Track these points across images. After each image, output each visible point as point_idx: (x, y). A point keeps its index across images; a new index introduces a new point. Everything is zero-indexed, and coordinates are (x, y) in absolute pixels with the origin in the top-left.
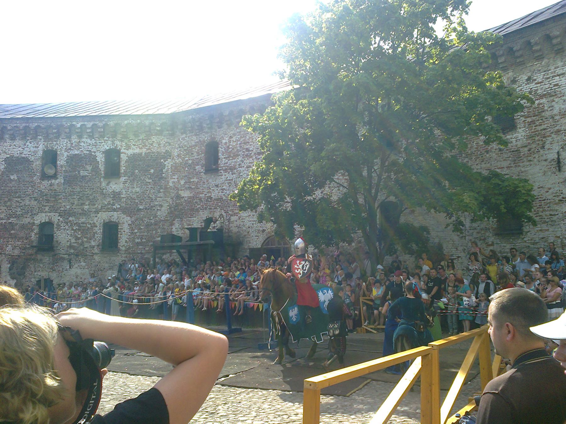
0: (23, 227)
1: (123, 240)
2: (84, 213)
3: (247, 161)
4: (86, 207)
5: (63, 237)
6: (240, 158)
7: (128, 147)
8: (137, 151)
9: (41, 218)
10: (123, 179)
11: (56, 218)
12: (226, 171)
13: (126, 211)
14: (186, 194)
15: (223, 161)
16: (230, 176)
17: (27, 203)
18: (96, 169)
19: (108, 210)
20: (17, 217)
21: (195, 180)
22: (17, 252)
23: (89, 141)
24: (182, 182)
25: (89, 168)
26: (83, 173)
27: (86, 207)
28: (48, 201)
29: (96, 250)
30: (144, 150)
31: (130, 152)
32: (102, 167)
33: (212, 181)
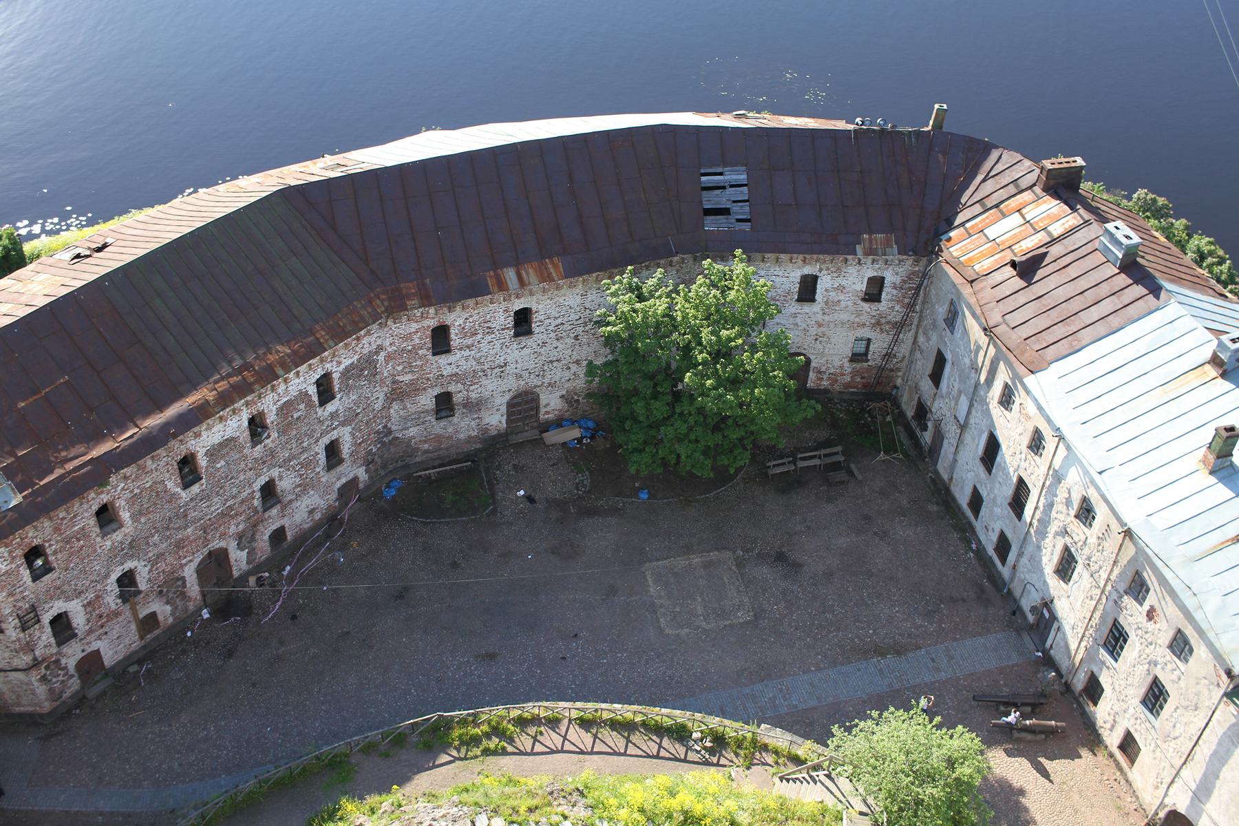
0: (243, 501)
1: (346, 449)
2: (305, 450)
3: (489, 338)
4: (305, 444)
5: (286, 483)
6: (479, 336)
7: (339, 363)
8: (347, 362)
9: (262, 480)
10: (338, 396)
11: (275, 473)
12: (461, 349)
13: (343, 424)
14: (407, 378)
15: (455, 340)
16: (467, 353)
17: (242, 477)
18: (310, 405)
19: (328, 433)
20: (234, 497)
21: (419, 363)
22: (241, 527)
23: (297, 381)
24: (400, 368)
25: (302, 406)
26: (295, 416)
27: (305, 444)
28: (264, 463)
29: (322, 474)
30: (356, 357)
31: (343, 367)
32: (315, 398)
33: (443, 360)
